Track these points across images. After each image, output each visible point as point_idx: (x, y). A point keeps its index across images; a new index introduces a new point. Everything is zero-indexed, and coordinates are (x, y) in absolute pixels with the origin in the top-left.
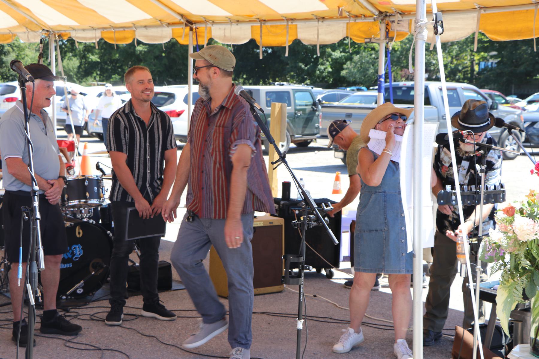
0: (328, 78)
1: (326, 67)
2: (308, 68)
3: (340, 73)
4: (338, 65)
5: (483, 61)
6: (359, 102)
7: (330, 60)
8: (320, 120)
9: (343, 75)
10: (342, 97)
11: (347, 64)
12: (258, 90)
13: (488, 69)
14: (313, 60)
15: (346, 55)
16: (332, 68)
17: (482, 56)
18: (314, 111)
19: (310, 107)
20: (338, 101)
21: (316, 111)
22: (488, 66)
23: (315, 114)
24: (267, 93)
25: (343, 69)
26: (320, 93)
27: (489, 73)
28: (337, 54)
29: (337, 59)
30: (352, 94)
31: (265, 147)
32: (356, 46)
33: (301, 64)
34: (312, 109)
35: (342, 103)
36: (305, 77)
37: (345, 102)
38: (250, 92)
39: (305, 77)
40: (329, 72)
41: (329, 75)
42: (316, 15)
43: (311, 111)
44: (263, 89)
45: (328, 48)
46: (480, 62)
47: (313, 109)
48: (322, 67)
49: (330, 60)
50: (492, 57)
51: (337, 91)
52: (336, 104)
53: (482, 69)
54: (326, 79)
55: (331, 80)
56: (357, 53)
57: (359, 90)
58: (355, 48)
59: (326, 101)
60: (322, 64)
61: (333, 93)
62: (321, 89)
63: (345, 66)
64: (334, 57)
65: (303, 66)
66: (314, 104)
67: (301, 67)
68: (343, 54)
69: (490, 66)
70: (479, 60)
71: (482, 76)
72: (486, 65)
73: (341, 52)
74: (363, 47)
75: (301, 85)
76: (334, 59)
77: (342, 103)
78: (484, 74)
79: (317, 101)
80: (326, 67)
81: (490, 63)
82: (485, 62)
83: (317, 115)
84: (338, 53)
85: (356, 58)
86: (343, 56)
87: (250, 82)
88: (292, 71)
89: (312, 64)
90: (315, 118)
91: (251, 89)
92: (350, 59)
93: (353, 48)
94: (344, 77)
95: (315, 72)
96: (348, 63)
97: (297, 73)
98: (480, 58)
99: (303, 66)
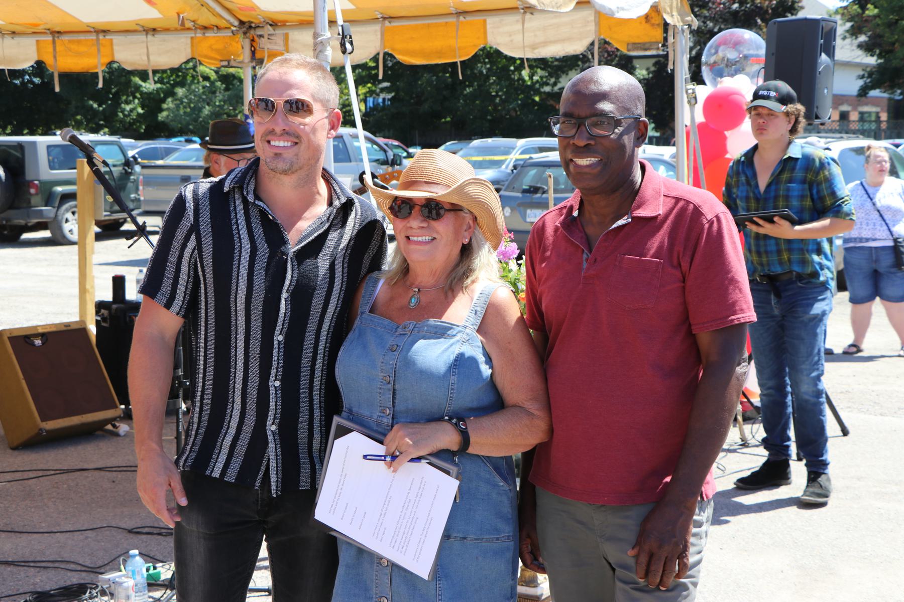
0: (138, 124)
1: (132, 108)
2: (104, 109)
3: (157, 117)
4: (153, 103)
5: (371, 96)
6: (194, 159)
7: (138, 95)
8: (141, 188)
9: (163, 120)
10: (168, 152)
11: (167, 102)
12: (34, 144)
13: (379, 109)
14: (111, 96)
15: (164, 87)
16: (142, 109)
17: (369, 88)
18: (126, 175)
19: (120, 168)
20: (162, 159)
21: (131, 174)
22: (378, 104)
23: (129, 179)
24: (49, 147)
25: (161, 110)
26: (134, 147)
27: (381, 114)
28: (149, 86)
29: (150, 94)
30: (183, 148)
31: (52, 233)
32: (180, 74)
33: (91, 102)
34: (124, 171)
35: (170, 161)
36: (102, 122)
37: (175, 160)
38: (20, 146)
39: (102, 122)
40: (139, 114)
41: (139, 119)
42: (93, 26)
43: (121, 173)
44: (42, 141)
45: (134, 76)
46: (366, 97)
47: (126, 170)
48: (128, 108)
49: (138, 95)
50: (382, 90)
51: (160, 144)
52: (160, 162)
53: (370, 107)
54: (135, 127)
55: (144, 127)
56: (182, 84)
57: (189, 141)
58: (178, 76)
59: (142, 159)
60: (127, 103)
61: (153, 146)
62: (133, 141)
63: (165, 106)
64: (145, 90)
65: (95, 106)
66: (127, 163)
67: (92, 106)
68: (159, 85)
69: (381, 104)
70: (365, 94)
71: (371, 119)
72: (375, 103)
73: (156, 82)
74: (190, 75)
75: (99, 135)
76: (146, 93)
77: (170, 161)
78: (374, 115)
79: (131, 159)
80: (132, 108)
81: (380, 100)
82: (374, 98)
83: (133, 180)
84: (150, 84)
85: (180, 92)
86: (160, 88)
87: (7, 132)
88: (77, 115)
89: (110, 102)
90: (130, 185)
91: (21, 142)
92: (171, 93)
93: (174, 77)
94: (163, 123)
95: (117, 115)
96: (170, 100)
97: (85, 117)
98: (368, 92)
99: (95, 106)
